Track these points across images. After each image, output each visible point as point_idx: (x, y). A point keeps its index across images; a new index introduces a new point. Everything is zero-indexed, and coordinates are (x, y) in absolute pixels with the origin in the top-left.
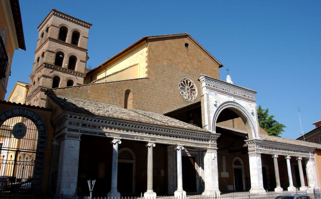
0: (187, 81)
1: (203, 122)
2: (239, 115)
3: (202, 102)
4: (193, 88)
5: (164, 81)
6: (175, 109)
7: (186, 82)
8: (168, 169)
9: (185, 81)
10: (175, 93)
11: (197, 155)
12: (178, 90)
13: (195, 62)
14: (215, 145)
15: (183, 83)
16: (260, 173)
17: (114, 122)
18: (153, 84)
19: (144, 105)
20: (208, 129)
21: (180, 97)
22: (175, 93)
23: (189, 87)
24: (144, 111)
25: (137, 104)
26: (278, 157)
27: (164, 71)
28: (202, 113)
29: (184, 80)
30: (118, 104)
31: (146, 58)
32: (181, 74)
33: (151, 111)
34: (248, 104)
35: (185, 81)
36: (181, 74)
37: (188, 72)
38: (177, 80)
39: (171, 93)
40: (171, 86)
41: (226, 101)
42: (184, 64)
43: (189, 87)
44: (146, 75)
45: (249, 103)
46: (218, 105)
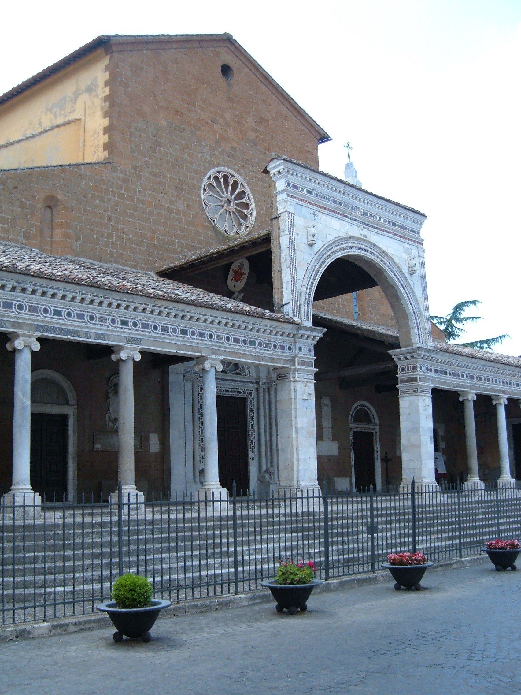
0: (226, 178)
1: (276, 295)
2: (375, 279)
3: (274, 237)
4: (243, 200)
5: (157, 175)
6: (192, 256)
7: (222, 180)
8: (172, 432)
9: (220, 176)
10: (192, 212)
11: (250, 393)
12: (200, 202)
13: (250, 122)
14: (311, 358)
15: (215, 184)
16: (429, 441)
17: (17, 284)
18: (125, 181)
19: (98, 244)
20: (291, 315)
21: (207, 224)
22: (192, 212)
23: (232, 195)
24: (100, 261)
25: (78, 239)
26: (475, 398)
27: (159, 144)
28: (275, 268)
29: (217, 174)
30: (21, 239)
31: (105, 101)
32: (208, 157)
33: (118, 263)
34: (402, 249)
35: (220, 176)
36: (208, 157)
37: (229, 150)
38: (195, 172)
39: (178, 212)
40: (180, 189)
41: (343, 235)
42: (217, 127)
43: (232, 195)
44: (106, 153)
45: (406, 245)
46: (319, 245)
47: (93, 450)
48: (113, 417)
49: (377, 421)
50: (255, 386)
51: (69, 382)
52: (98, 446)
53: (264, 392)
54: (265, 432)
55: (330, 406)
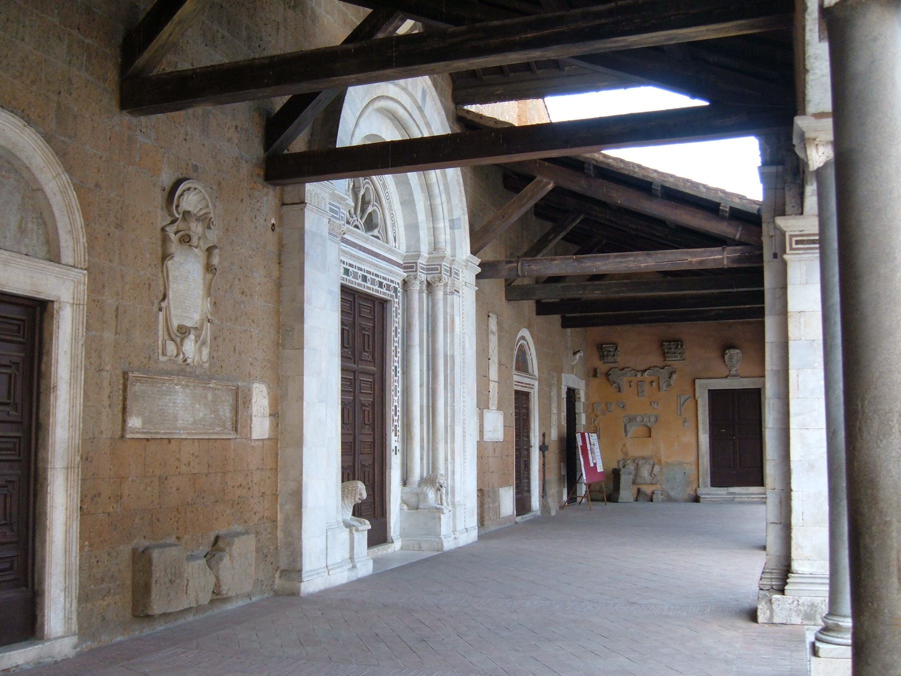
8: (307, 379)
11: (395, 290)
47: (122, 437)
48: (175, 323)
49: (536, 373)
50: (400, 275)
51: (65, 177)
52: (135, 422)
53: (421, 292)
54: (421, 385)
55: (496, 334)
